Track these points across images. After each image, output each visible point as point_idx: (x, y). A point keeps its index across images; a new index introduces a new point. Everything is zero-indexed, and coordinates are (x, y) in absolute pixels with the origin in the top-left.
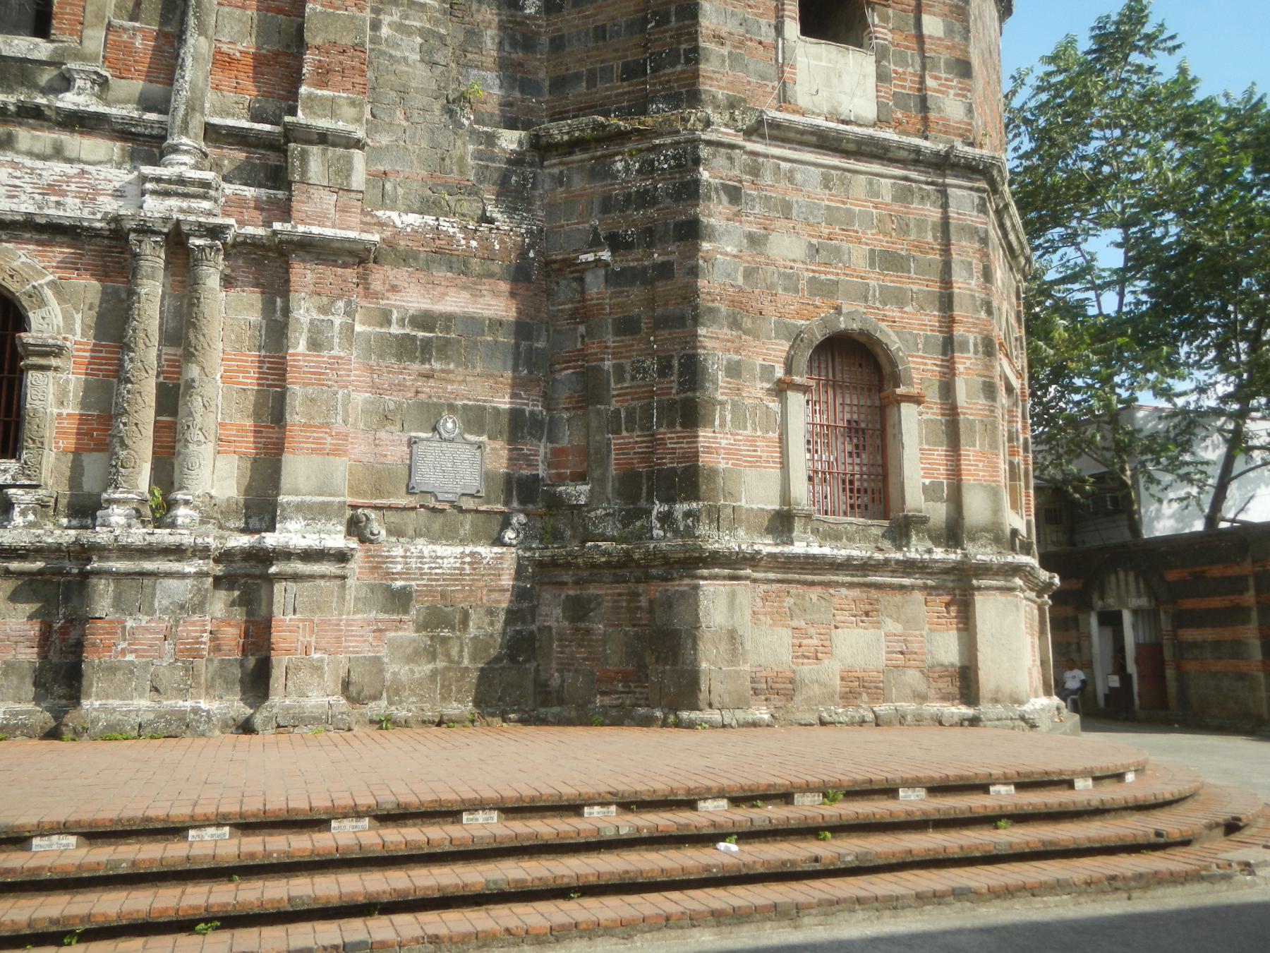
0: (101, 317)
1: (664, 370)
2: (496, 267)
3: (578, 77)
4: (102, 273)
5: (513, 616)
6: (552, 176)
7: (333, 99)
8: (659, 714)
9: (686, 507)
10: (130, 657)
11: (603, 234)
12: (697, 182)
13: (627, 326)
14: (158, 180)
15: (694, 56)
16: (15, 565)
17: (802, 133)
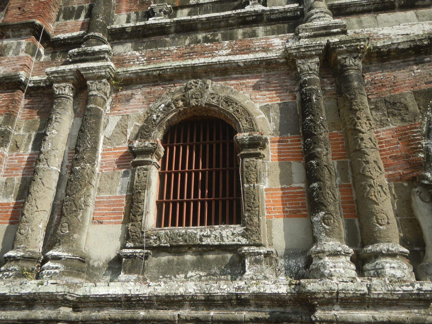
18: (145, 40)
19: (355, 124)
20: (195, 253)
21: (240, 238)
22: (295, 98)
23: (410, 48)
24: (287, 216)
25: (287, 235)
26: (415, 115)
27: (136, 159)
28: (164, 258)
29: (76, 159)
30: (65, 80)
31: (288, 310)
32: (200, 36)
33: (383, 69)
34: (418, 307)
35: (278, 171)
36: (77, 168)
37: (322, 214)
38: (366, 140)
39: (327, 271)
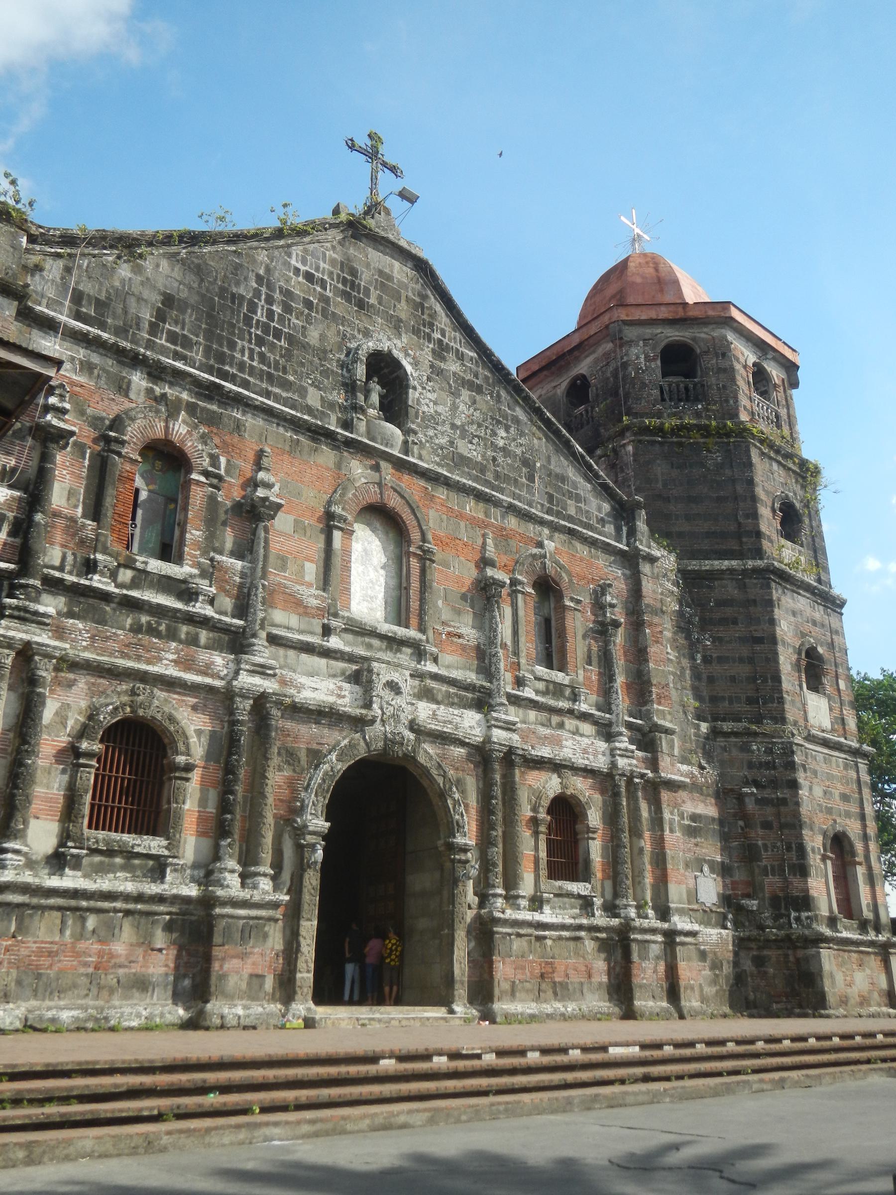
0: (604, 813)
1: (789, 848)
2: (711, 791)
3: (723, 698)
4: (603, 792)
5: (736, 964)
6: (721, 747)
7: (663, 711)
8: (810, 1012)
9: (806, 914)
10: (645, 981)
11: (750, 779)
12: (794, 762)
13: (767, 825)
14: (620, 749)
15: (781, 701)
16: (598, 935)
17: (820, 739)
18: (82, 599)
19: (265, 771)
20: (123, 858)
21: (164, 850)
22: (223, 728)
23: (316, 710)
24: (199, 836)
25: (197, 850)
26: (303, 770)
27: (81, 761)
28: (97, 859)
29: (27, 751)
30: (9, 646)
31: (191, 907)
32: (144, 619)
33: (292, 719)
34: (272, 909)
35: (197, 795)
36: (30, 762)
37: (229, 840)
38: (269, 786)
39: (226, 883)
